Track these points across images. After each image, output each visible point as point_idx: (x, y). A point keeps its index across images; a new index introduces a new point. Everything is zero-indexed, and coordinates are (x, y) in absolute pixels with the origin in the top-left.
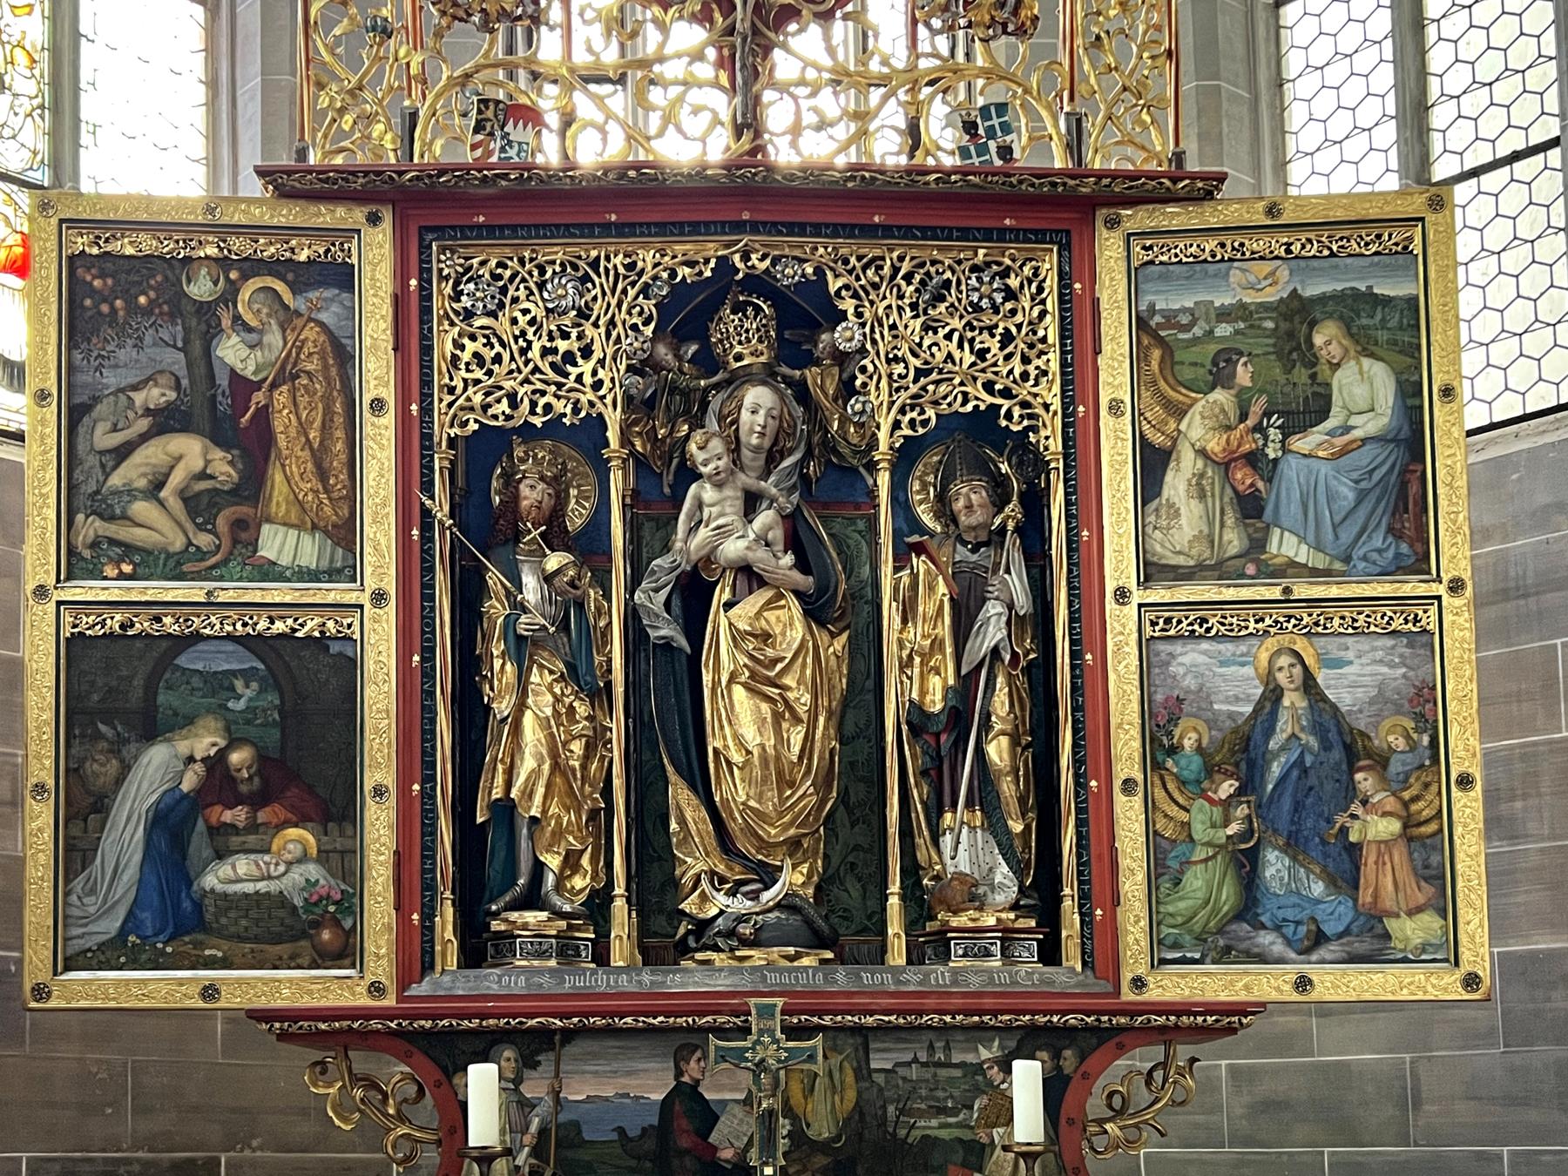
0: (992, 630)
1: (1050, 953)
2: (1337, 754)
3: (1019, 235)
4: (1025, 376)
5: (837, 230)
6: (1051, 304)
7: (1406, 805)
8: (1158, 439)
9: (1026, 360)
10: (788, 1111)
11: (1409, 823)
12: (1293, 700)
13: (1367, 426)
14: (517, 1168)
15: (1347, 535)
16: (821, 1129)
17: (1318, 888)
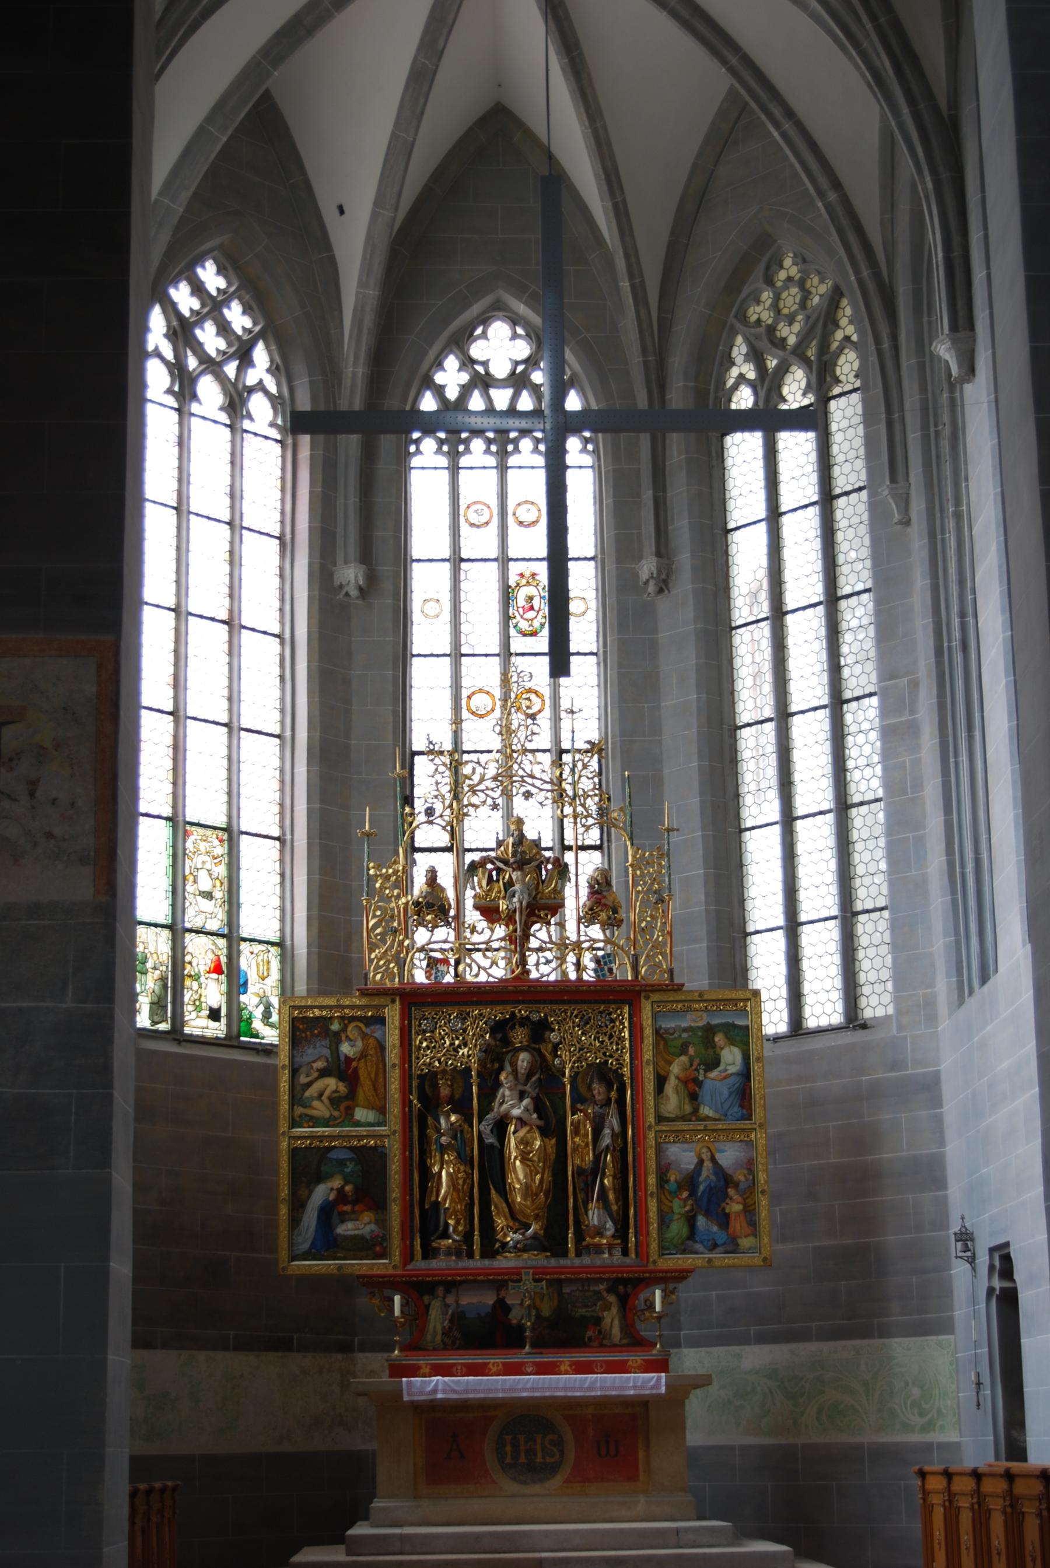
0: (606, 1141)
1: (625, 1252)
2: (722, 1182)
3: (614, 1002)
4: (617, 1050)
5: (552, 1002)
6: (626, 1024)
7: (744, 1199)
8: (662, 1073)
9: (617, 1044)
11: (745, 1206)
12: (708, 1164)
13: (732, 1069)
15: (726, 1106)
16: (546, 1312)
17: (715, 1228)
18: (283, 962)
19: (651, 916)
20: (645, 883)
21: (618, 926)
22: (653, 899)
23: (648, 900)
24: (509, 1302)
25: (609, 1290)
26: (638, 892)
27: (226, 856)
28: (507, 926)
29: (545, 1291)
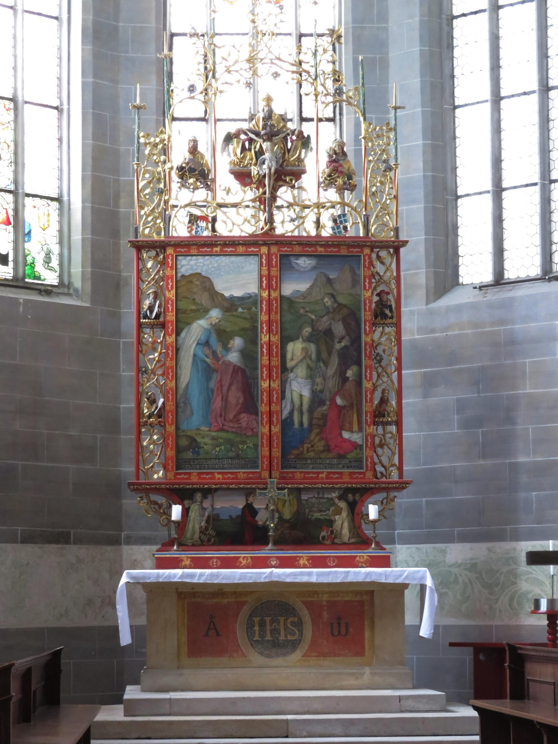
10: (278, 511)
14: (201, 526)
16: (287, 515)
18: (61, 215)
19: (381, 183)
20: (375, 154)
21: (352, 191)
22: (382, 167)
23: (378, 168)
24: (256, 506)
25: (340, 498)
26: (370, 161)
27: (12, 123)
28: (258, 189)
29: (286, 498)
